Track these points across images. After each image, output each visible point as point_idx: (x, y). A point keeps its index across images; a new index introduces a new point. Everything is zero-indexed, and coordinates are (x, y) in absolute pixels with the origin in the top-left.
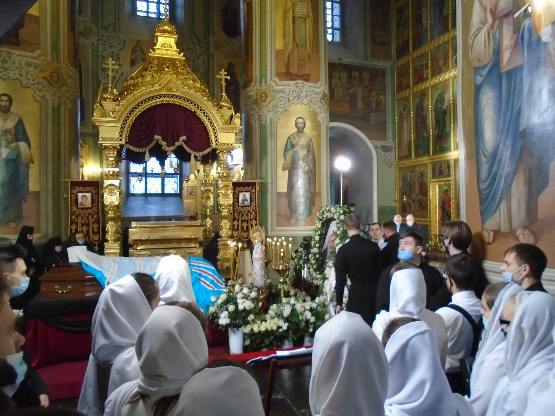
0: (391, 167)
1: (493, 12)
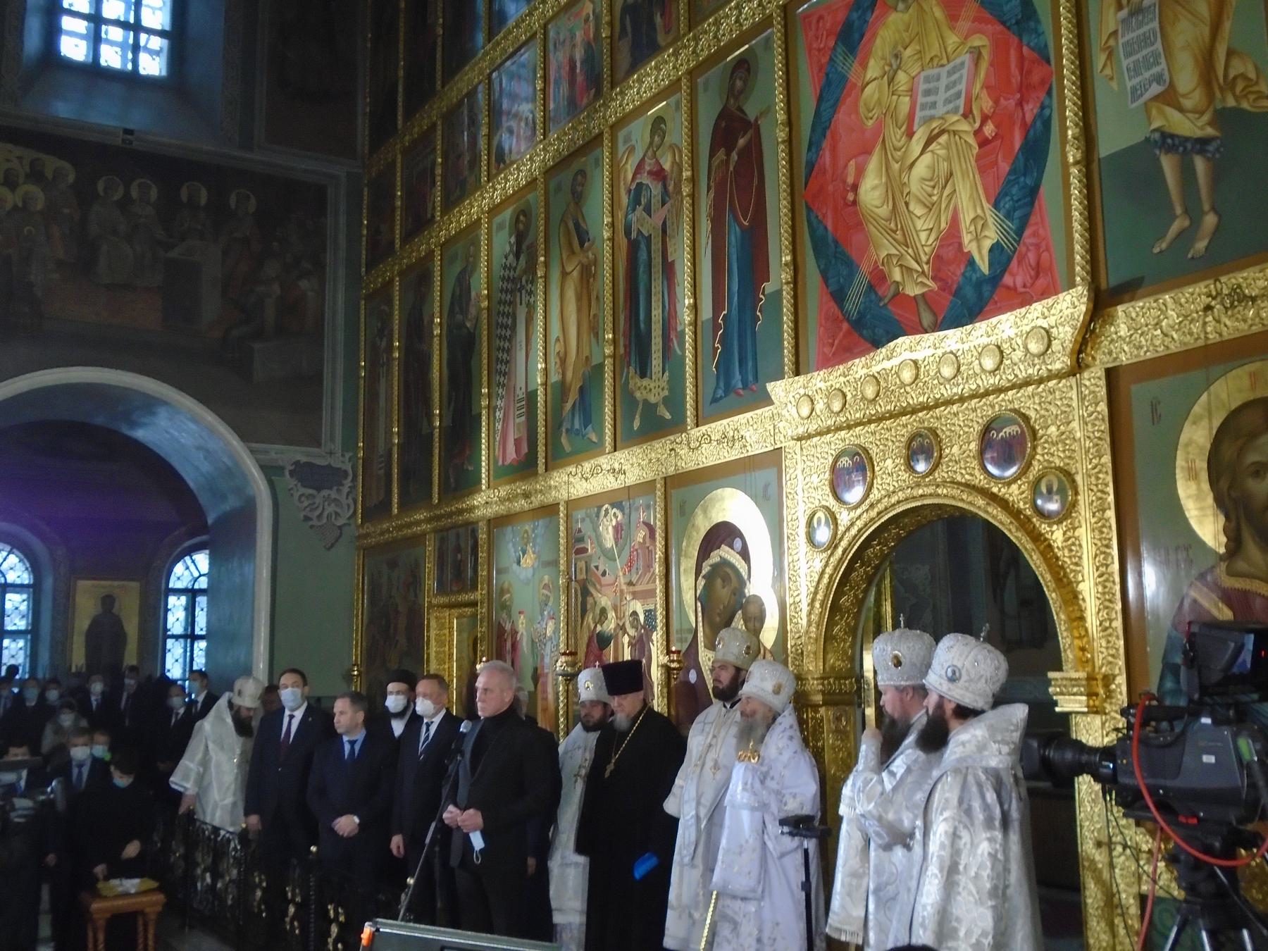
0: (332, 545)
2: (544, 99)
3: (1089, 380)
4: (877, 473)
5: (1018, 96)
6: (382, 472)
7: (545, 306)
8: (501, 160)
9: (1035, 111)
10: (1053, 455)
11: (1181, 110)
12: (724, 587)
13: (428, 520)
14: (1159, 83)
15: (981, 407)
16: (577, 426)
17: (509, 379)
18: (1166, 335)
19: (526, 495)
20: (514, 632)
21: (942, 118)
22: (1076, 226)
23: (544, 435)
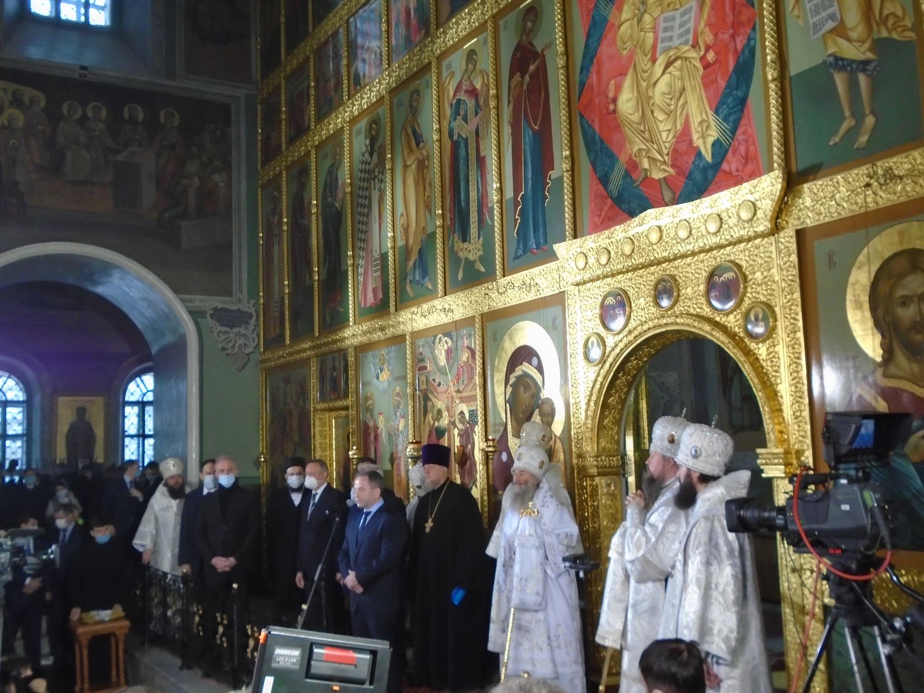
0: (243, 368)
2: (388, 38)
3: (784, 238)
4: (633, 308)
5: (731, 31)
6: (277, 314)
7: (392, 190)
8: (357, 83)
9: (744, 42)
10: (758, 293)
11: (849, 40)
12: (525, 392)
13: (312, 348)
14: (833, 21)
15: (707, 260)
16: (417, 278)
17: (367, 244)
18: (838, 205)
19: (382, 329)
20: (376, 428)
21: (677, 48)
22: (774, 126)
23: (393, 285)
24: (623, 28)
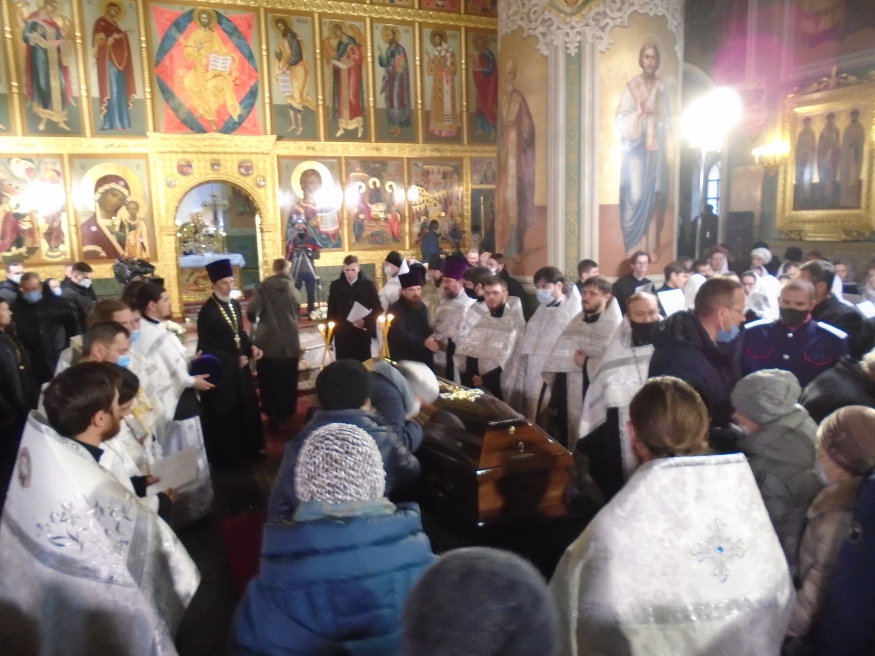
1: (643, 105)
24: (189, 50)
